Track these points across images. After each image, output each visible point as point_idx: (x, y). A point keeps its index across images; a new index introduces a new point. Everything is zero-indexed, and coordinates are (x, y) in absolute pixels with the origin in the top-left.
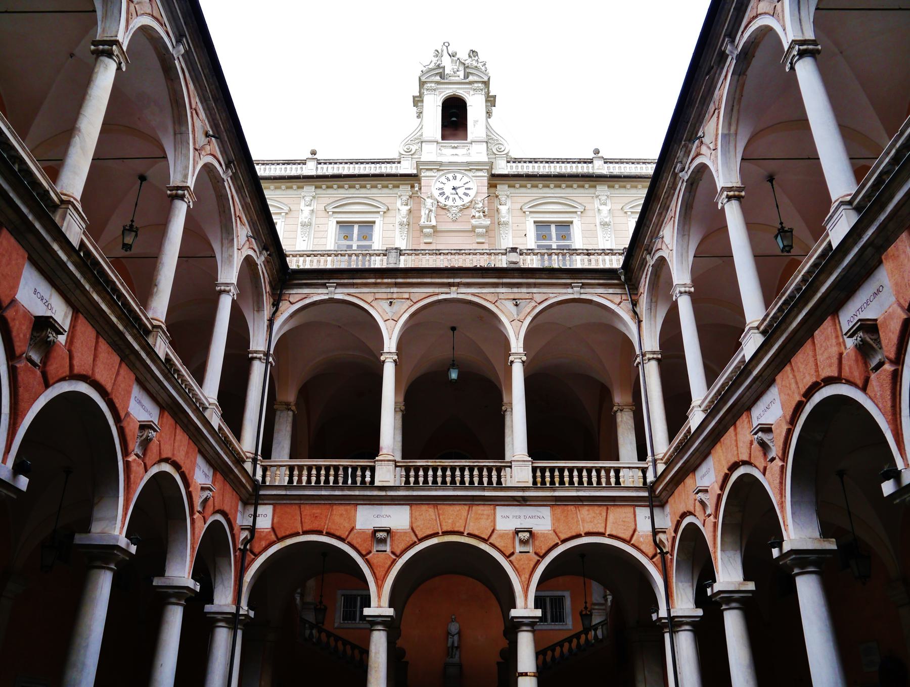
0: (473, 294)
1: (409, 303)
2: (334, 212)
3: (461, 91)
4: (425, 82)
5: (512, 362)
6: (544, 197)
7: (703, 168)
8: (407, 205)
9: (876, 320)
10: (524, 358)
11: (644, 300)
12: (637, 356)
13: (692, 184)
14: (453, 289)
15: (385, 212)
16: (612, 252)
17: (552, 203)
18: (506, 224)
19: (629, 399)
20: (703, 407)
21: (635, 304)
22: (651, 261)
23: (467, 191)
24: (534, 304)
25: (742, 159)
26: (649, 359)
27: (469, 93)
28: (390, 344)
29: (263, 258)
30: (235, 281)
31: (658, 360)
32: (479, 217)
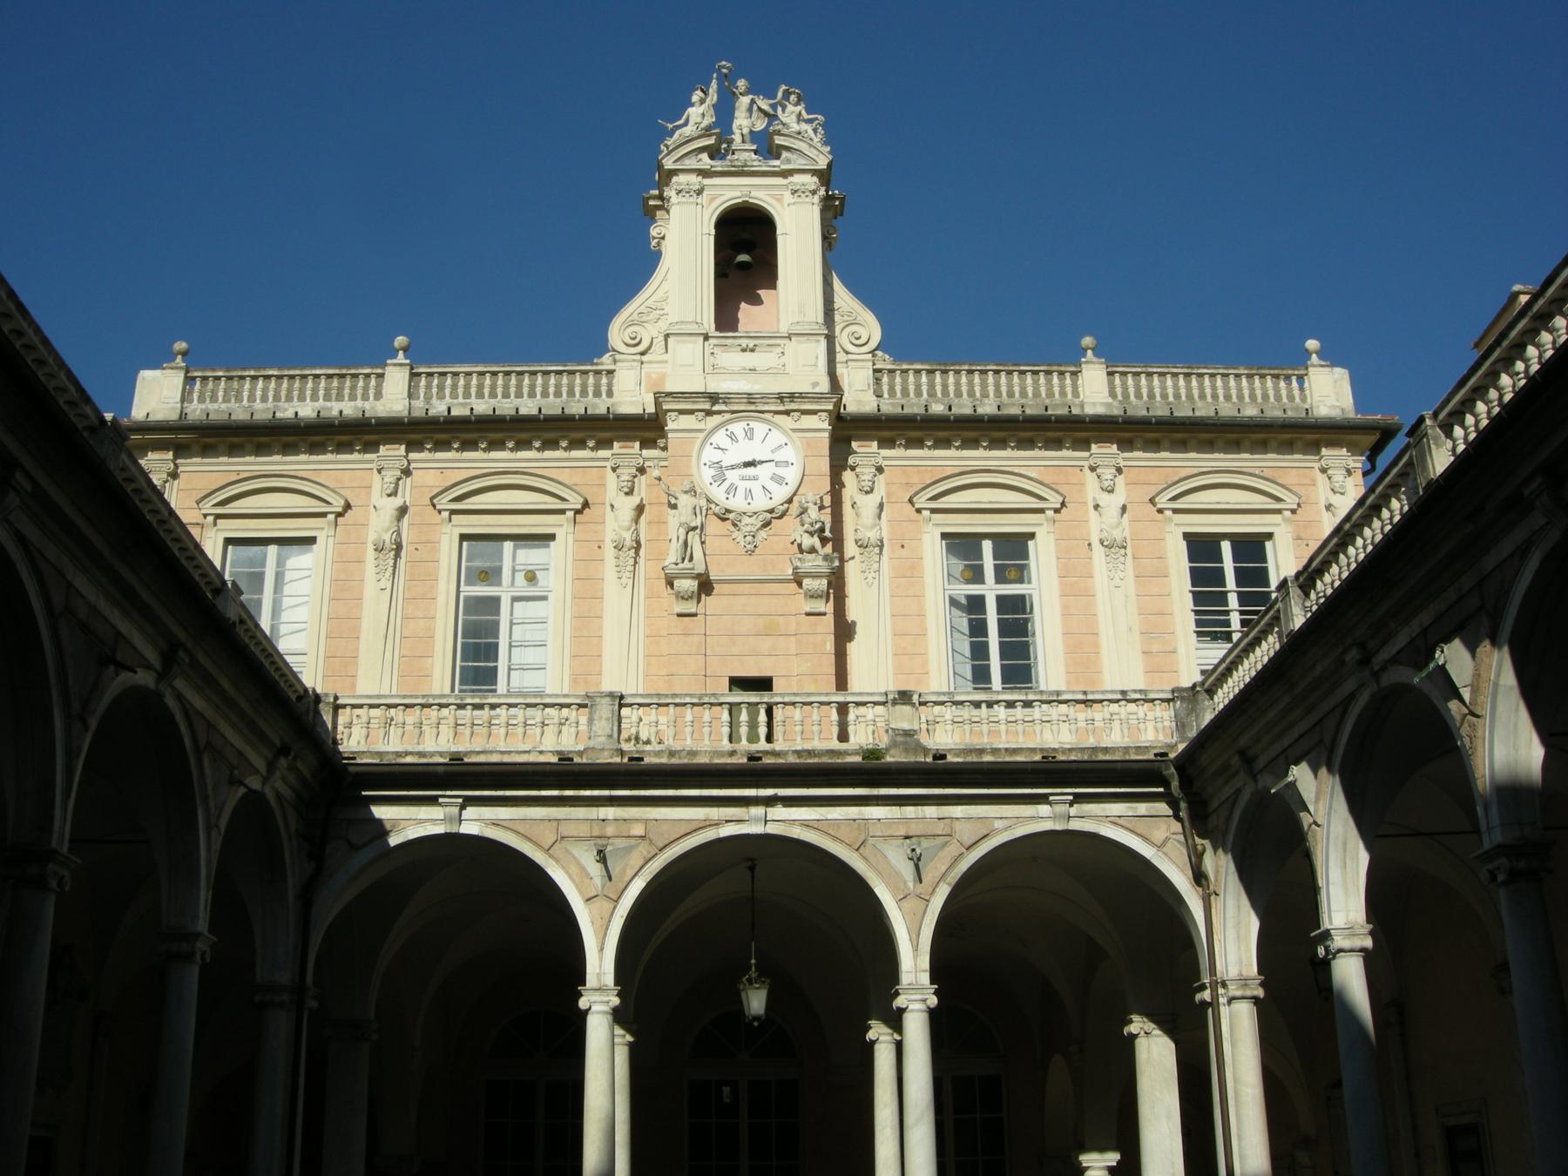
0: (806, 824)
2: (453, 512)
4: (675, 172)
12: (1202, 988)
14: (757, 811)
15: (578, 512)
23: (781, 471)
24: (953, 849)
27: (779, 199)
28: (600, 963)
32: (812, 550)
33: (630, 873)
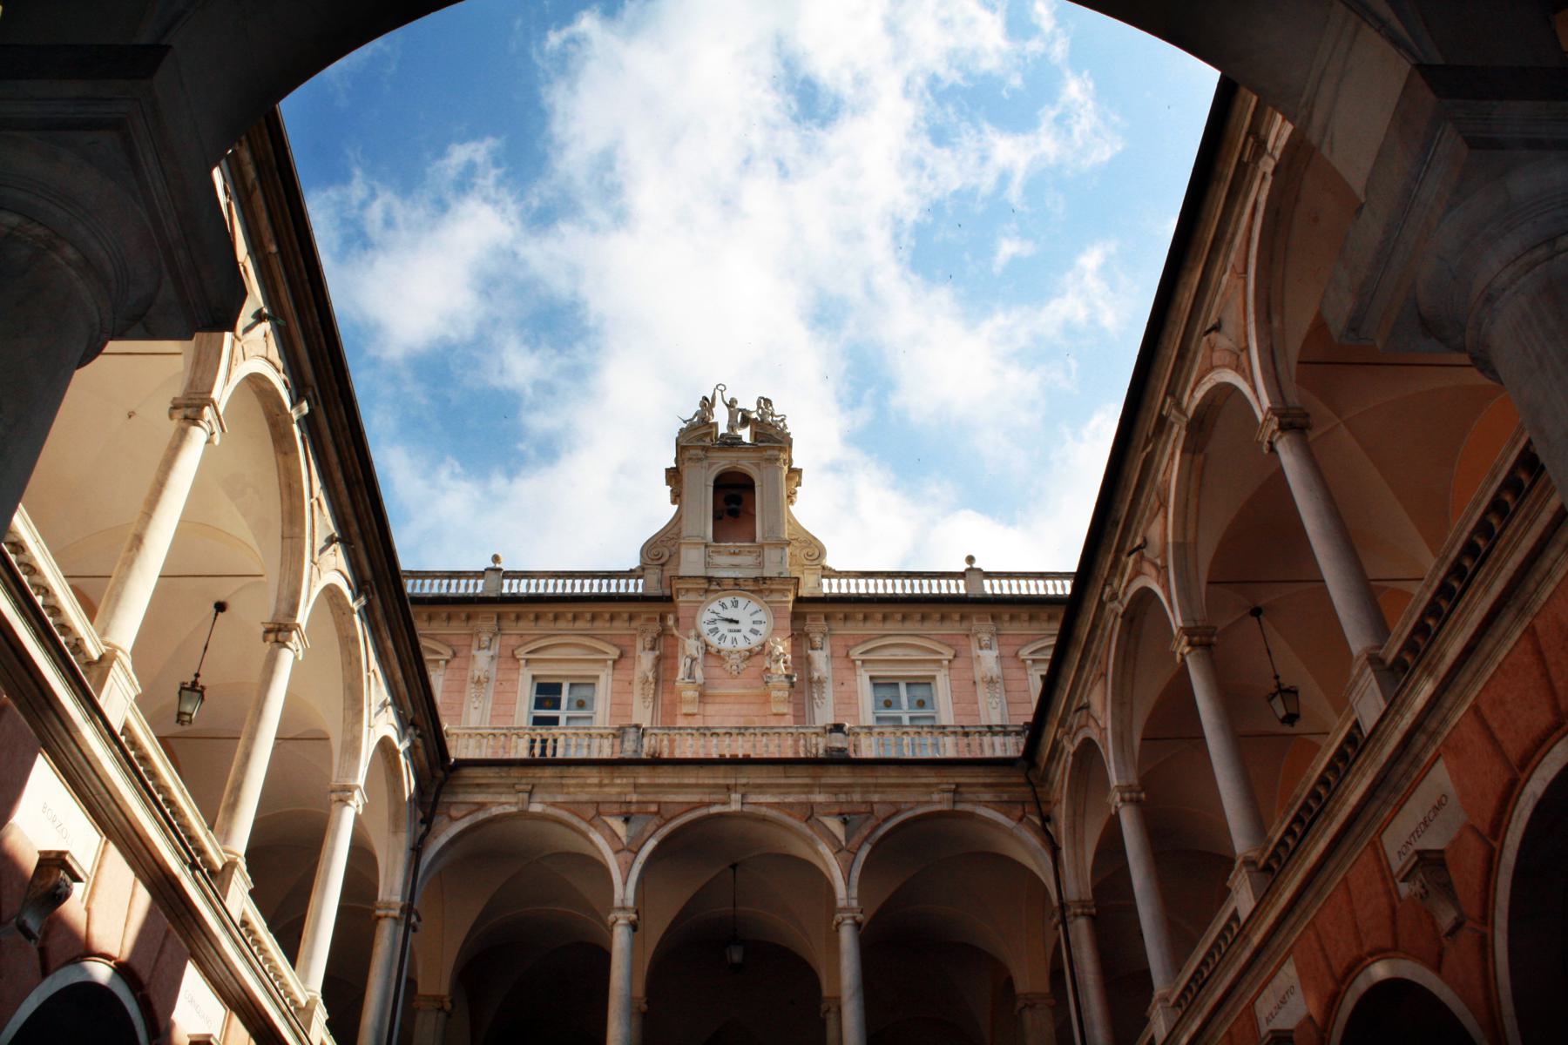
0: (769, 805)
1: (656, 820)
3: (744, 462)
5: (839, 924)
6: (885, 636)
7: (1146, 595)
8: (653, 649)
9: (1441, 852)
10: (860, 917)
11: (1062, 813)
13: (1132, 620)
16: (1004, 731)
17: (902, 647)
18: (820, 681)
19: (1042, 985)
20: (1173, 999)
21: (1046, 819)
22: (1070, 748)
24: (872, 822)
25: (1209, 583)
26: (1076, 916)
27: (758, 465)
28: (624, 891)
29: (406, 743)
30: (361, 780)
31: (1090, 916)
33: (647, 834)
